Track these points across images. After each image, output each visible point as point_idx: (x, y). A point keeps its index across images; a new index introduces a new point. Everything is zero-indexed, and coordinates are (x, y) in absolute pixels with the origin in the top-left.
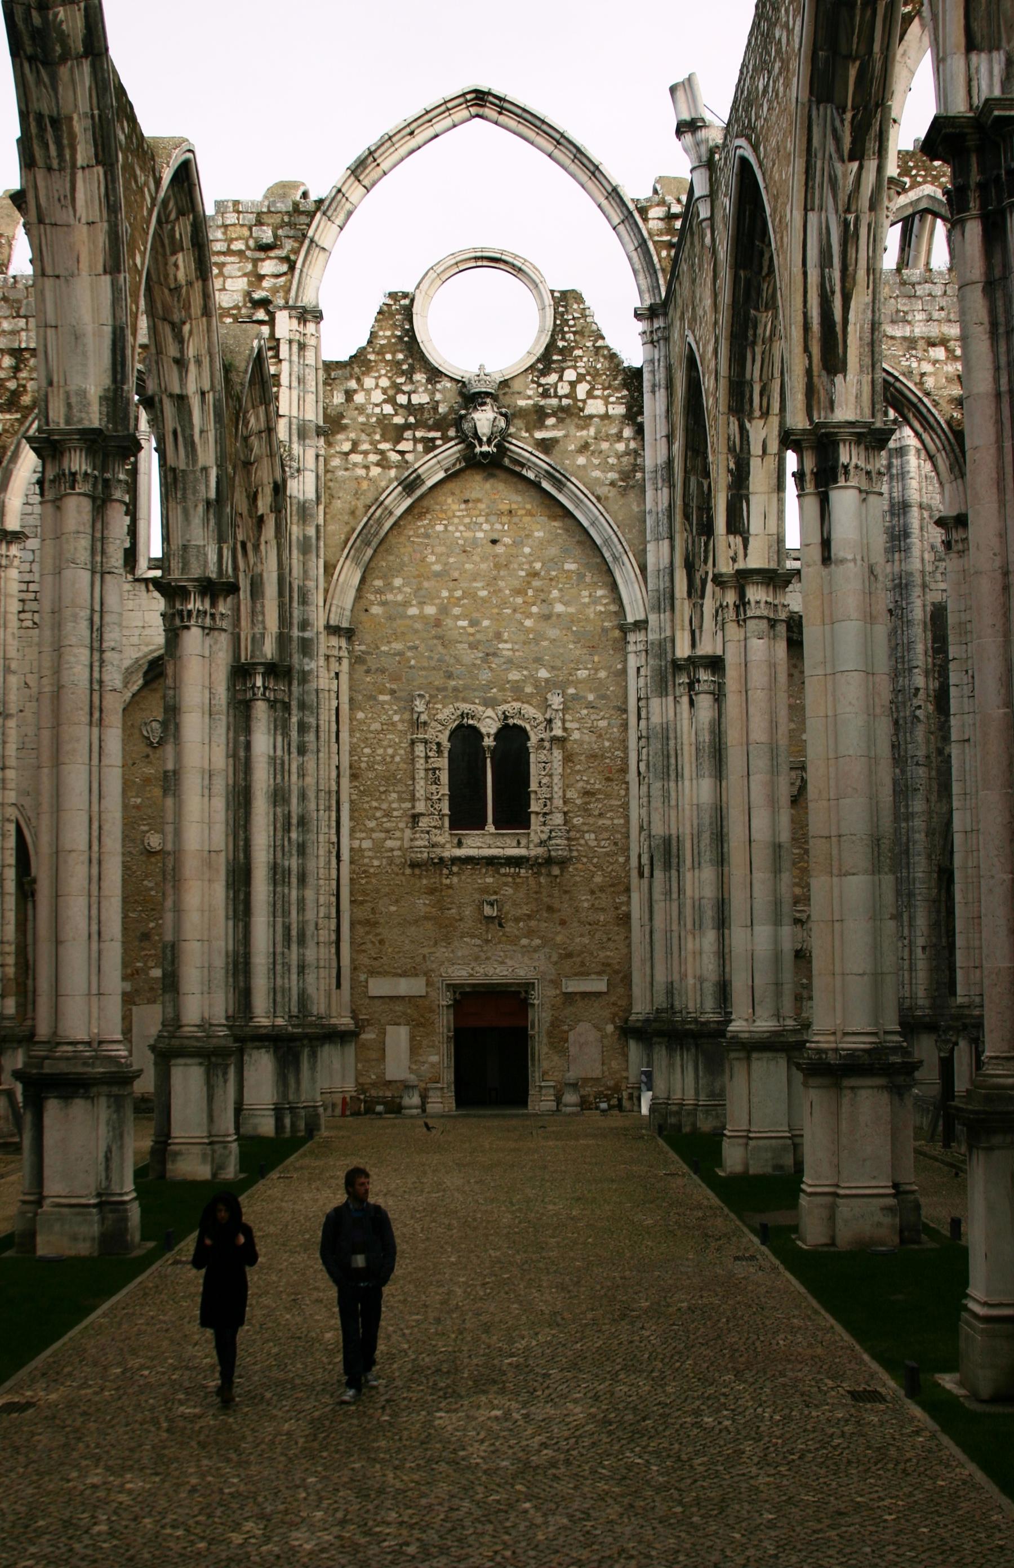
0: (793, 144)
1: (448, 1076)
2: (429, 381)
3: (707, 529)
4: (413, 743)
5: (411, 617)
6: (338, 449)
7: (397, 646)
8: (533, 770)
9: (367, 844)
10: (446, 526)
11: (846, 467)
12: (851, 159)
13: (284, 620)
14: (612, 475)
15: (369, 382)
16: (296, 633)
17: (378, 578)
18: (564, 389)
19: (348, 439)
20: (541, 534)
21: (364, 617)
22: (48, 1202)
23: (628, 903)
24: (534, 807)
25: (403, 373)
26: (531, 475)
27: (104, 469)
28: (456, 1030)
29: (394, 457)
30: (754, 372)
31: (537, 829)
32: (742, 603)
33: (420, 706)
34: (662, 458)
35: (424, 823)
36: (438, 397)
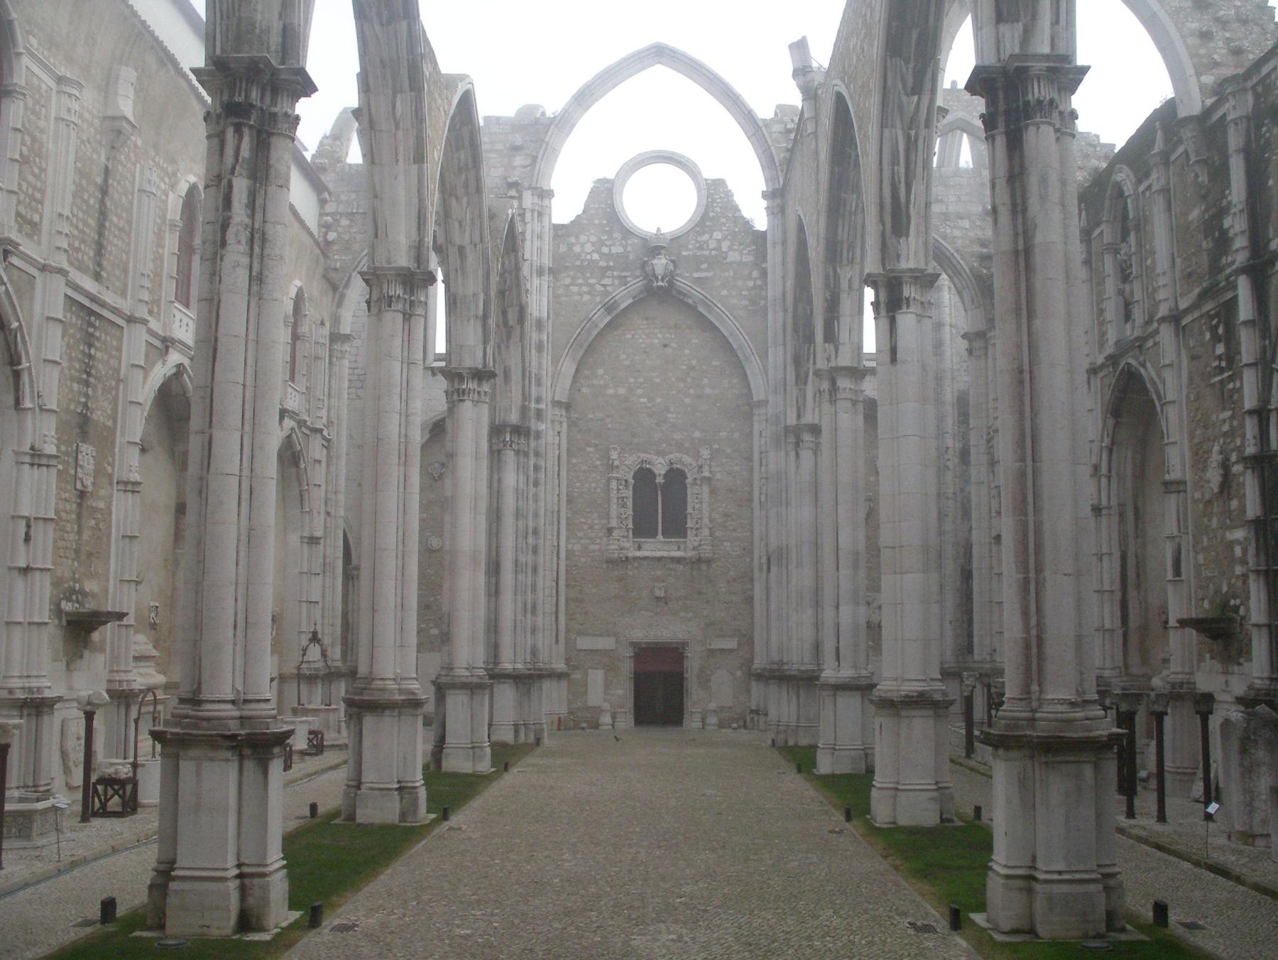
0: (875, 84)
1: (630, 704)
2: (623, 238)
3: (810, 339)
4: (609, 480)
7: (600, 415)
8: (689, 500)
9: (577, 547)
11: (908, 299)
12: (913, 94)
13: (525, 397)
14: (745, 302)
15: (583, 238)
16: (533, 405)
18: (712, 245)
22: (364, 787)
23: (752, 589)
24: (689, 524)
26: (690, 301)
27: (412, 294)
28: (635, 673)
29: (599, 288)
30: (842, 234)
31: (692, 539)
32: (834, 389)
33: (614, 455)
34: (779, 290)
35: (616, 534)
36: (629, 248)
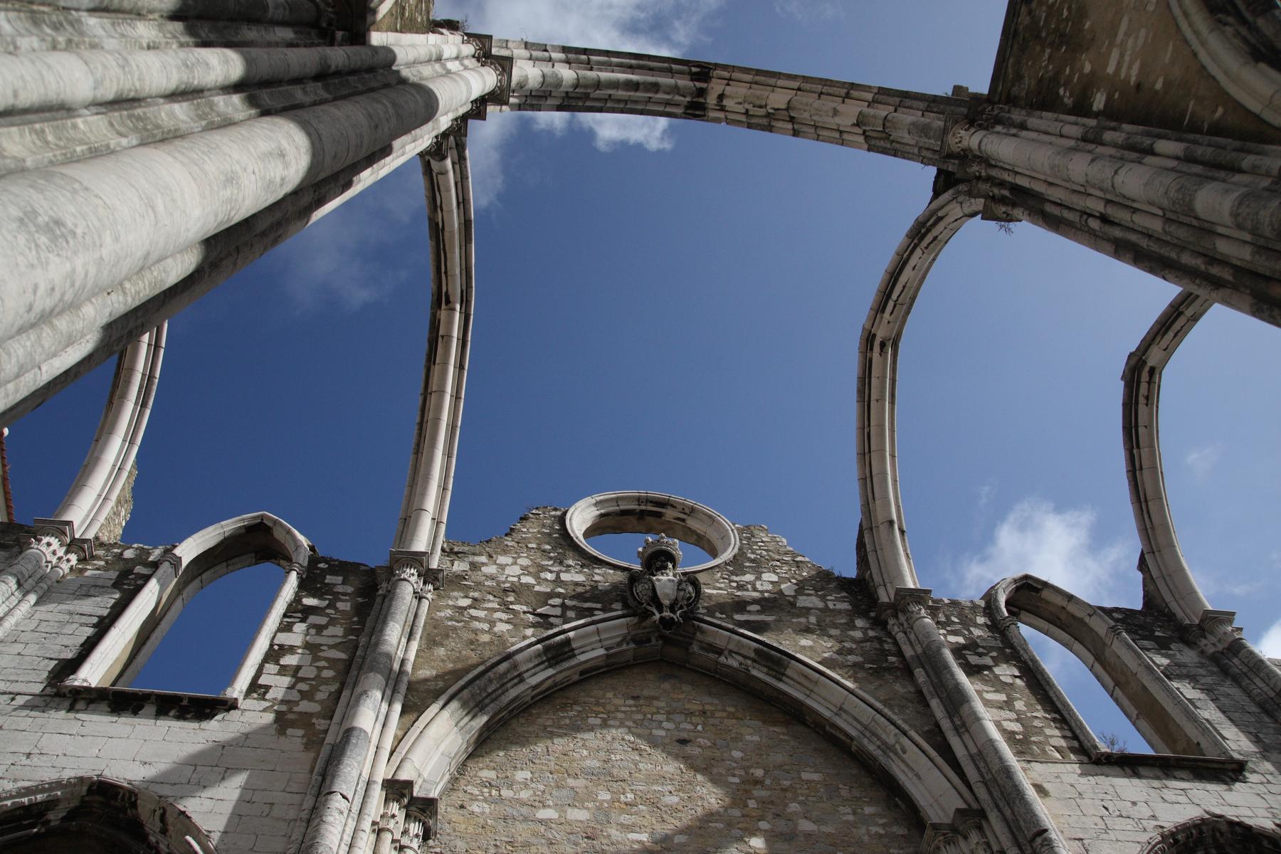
5: (541, 822)
6: (450, 603)
10: (604, 720)
15: (502, 560)
17: (488, 767)
19: (467, 597)
20: (756, 738)
21: (454, 815)
25: (551, 558)
26: (733, 662)
